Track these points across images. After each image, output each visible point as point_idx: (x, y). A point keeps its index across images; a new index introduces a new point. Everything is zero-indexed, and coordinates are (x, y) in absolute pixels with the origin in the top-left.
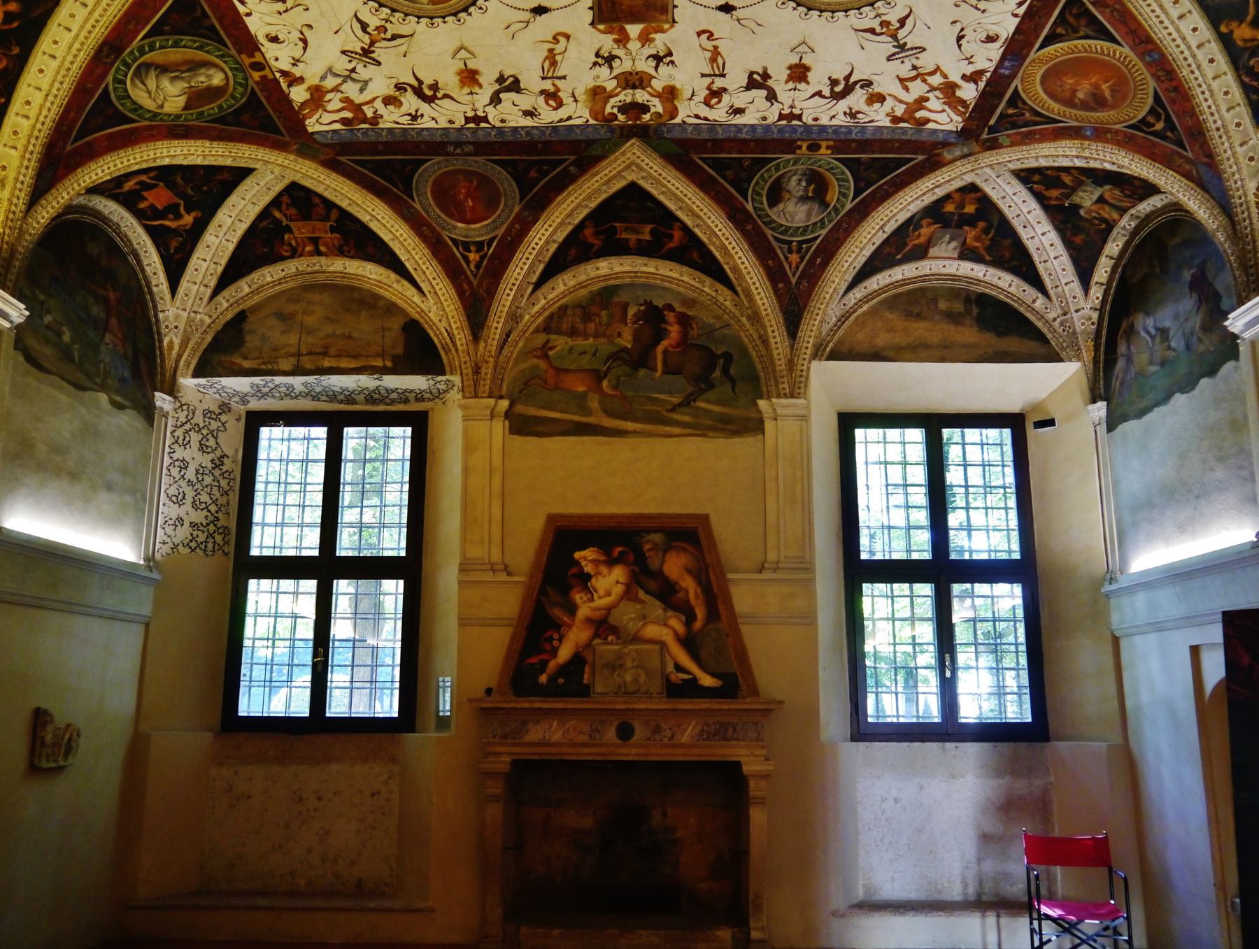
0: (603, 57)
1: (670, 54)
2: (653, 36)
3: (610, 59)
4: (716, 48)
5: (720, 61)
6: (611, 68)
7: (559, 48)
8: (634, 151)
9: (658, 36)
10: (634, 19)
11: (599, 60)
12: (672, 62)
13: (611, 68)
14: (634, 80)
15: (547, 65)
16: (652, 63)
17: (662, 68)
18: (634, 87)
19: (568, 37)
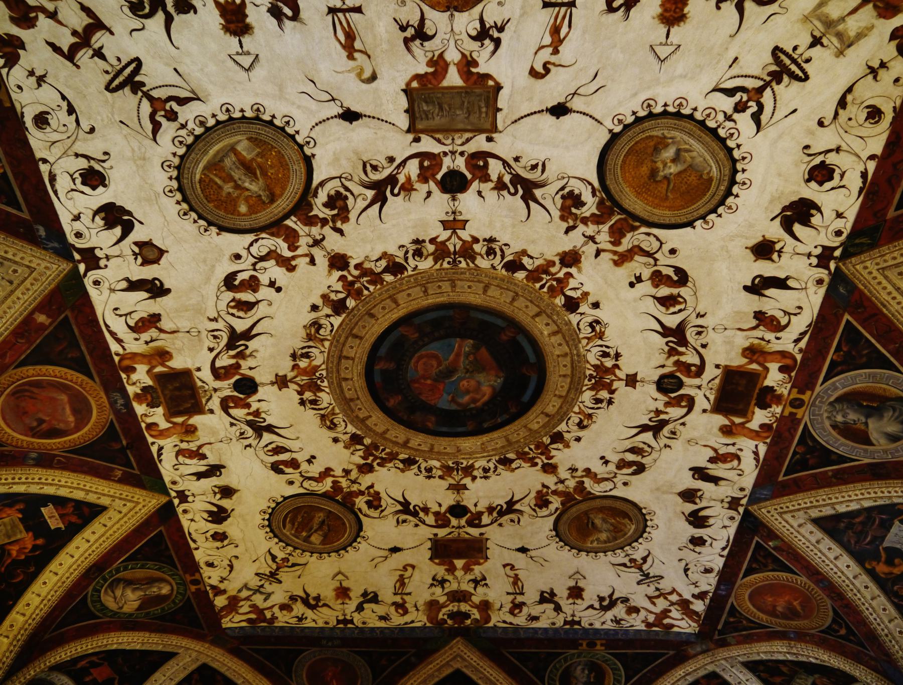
0: (492, 39)
1: (407, 41)
2: (431, 70)
3: (482, 35)
4: (351, 57)
5: (342, 38)
6: (482, 21)
7: (546, 55)
8: (458, 646)
9: (423, 69)
10: (459, 557)
11: (496, 34)
12: (403, 29)
13: (482, 21)
14: (459, 596)
15: (564, 31)
16: (429, 30)
17: (415, 20)
18: (459, 601)
19: (533, 73)
